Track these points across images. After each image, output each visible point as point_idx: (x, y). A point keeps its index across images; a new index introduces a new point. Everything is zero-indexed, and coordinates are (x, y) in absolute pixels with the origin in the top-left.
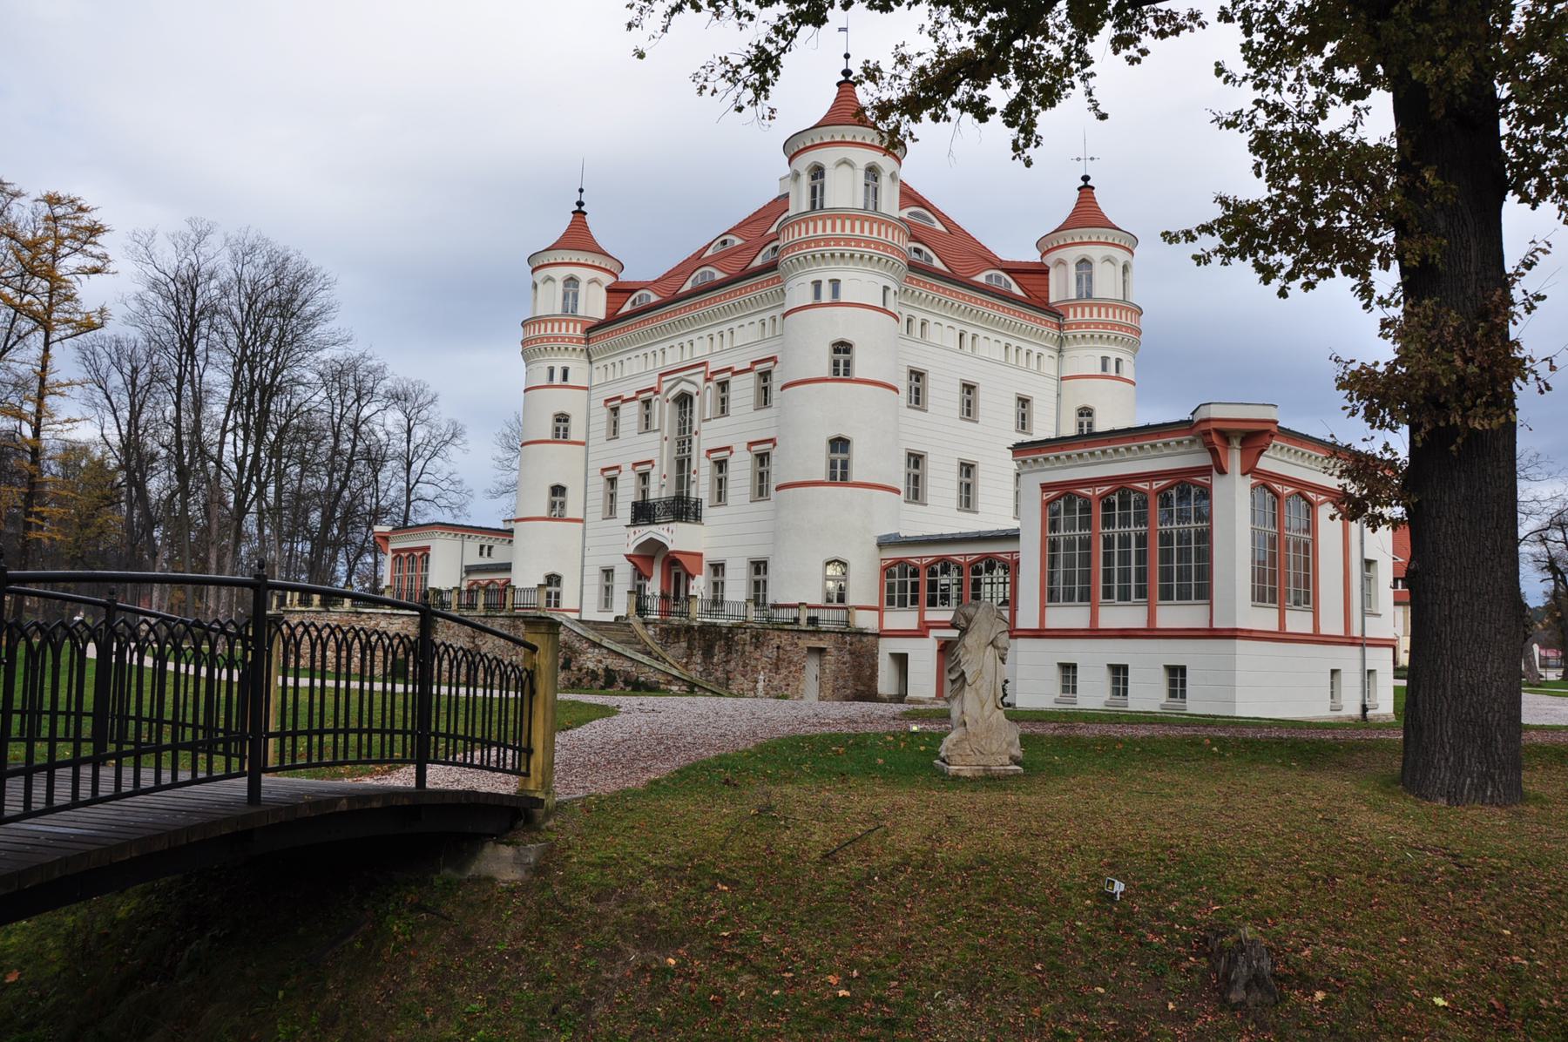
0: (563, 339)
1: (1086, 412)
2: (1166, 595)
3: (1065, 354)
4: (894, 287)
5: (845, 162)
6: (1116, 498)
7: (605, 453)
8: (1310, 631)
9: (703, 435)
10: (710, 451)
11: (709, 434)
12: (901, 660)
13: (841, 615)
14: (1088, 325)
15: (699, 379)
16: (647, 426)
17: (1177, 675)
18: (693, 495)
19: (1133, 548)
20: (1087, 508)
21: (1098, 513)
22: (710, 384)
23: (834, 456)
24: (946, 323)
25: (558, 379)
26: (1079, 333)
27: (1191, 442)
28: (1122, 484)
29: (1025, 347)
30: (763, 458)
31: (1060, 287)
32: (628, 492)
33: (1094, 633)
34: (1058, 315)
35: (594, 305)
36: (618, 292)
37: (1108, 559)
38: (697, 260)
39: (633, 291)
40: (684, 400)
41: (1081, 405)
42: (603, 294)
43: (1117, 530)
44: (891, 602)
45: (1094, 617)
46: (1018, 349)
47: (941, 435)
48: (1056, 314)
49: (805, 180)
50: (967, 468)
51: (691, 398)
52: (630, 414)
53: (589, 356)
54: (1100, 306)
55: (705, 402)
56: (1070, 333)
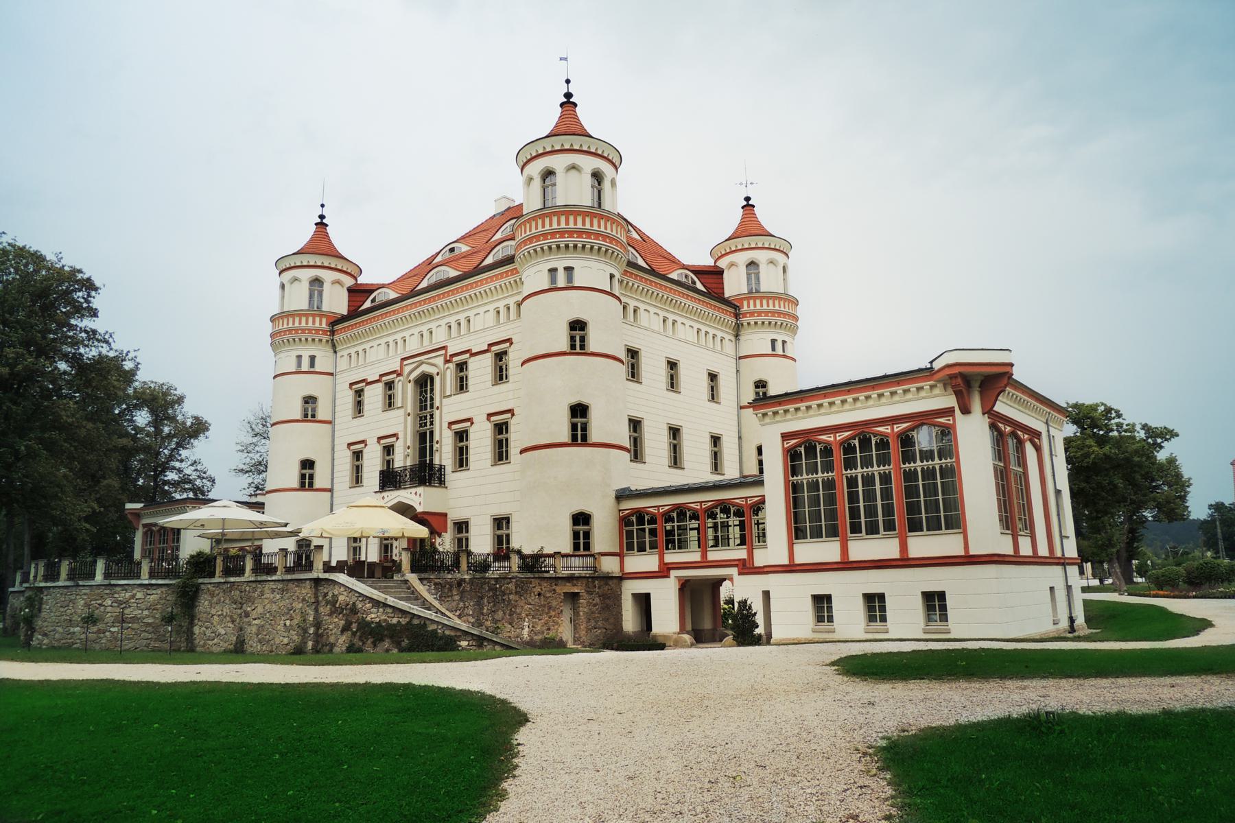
0: (310, 331)
1: (761, 384)
2: (915, 526)
3: (742, 338)
4: (617, 275)
5: (573, 167)
6: (856, 442)
7: (349, 429)
8: (1031, 554)
9: (444, 409)
10: (451, 424)
11: (449, 408)
12: (644, 602)
13: (588, 561)
14: (759, 313)
15: (440, 361)
16: (389, 403)
17: (935, 602)
18: (436, 461)
19: (878, 487)
20: (827, 451)
21: (838, 457)
22: (450, 365)
23: (575, 420)
24: (653, 310)
25: (305, 366)
26: (752, 320)
27: (932, 387)
29: (712, 331)
30: (501, 428)
31: (734, 284)
32: (373, 464)
33: (846, 565)
34: (735, 307)
35: (336, 301)
36: (358, 293)
37: (853, 497)
38: (430, 264)
39: (372, 291)
40: (424, 383)
41: (757, 378)
42: (346, 294)
43: (859, 471)
44: (630, 547)
45: (844, 550)
46: (707, 333)
47: (653, 403)
48: (733, 306)
49: (537, 182)
50: (675, 432)
52: (374, 395)
53: (334, 346)
54: (761, 298)
55: (445, 380)
56: (744, 320)
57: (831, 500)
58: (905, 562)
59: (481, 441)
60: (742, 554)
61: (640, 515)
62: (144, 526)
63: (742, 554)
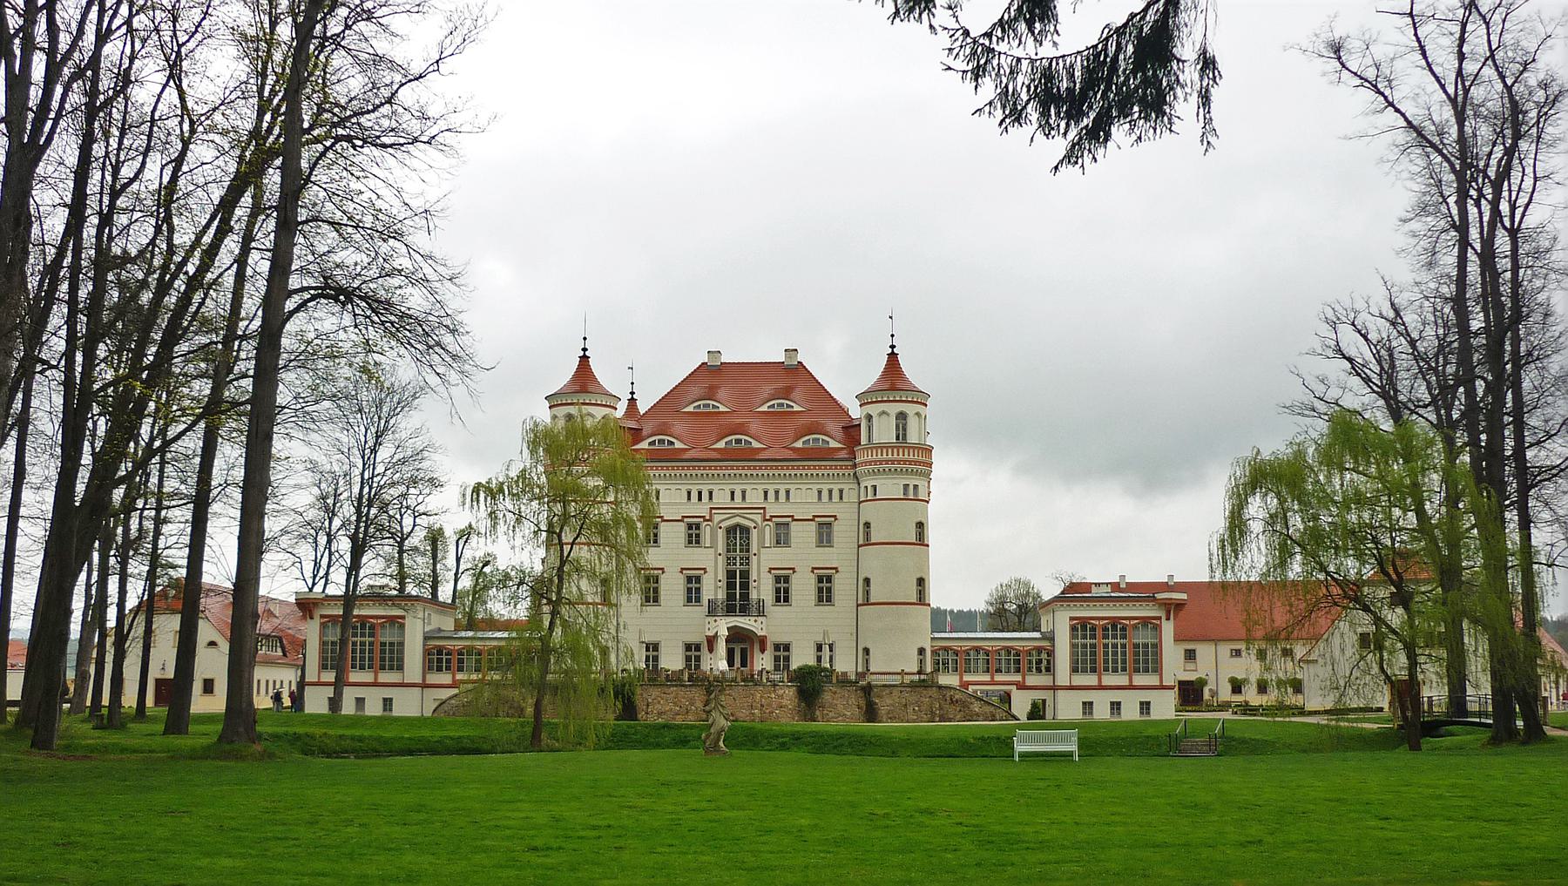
2: (1137, 670)
15: (758, 518)
18: (754, 595)
20: (1093, 629)
21: (1099, 633)
28: (1115, 622)
33: (1101, 687)
51: (746, 531)
57: (1093, 654)
58: (1131, 687)
59: (804, 587)
60: (1018, 678)
61: (946, 649)
62: (322, 616)
63: (1018, 678)
